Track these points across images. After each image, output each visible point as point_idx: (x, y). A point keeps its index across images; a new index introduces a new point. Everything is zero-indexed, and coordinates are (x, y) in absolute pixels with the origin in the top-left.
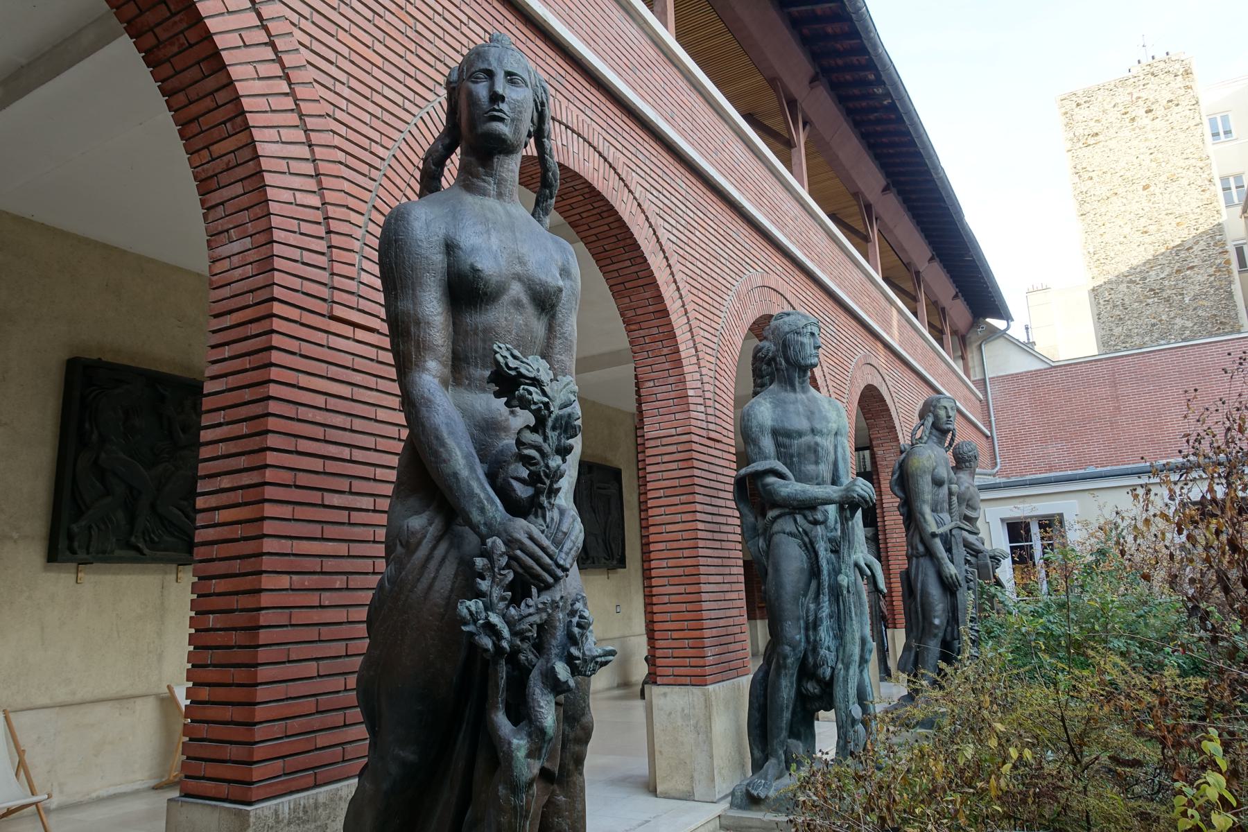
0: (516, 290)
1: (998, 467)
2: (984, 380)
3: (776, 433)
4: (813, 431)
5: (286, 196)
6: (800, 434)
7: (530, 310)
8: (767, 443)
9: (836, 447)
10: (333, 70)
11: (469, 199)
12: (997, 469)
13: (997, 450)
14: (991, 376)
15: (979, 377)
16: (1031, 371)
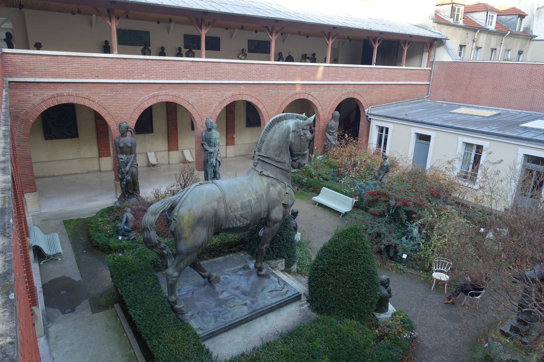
0: (125, 147)
1: (428, 96)
2: (433, 61)
3: (205, 138)
4: (210, 138)
5: (113, 128)
6: (208, 139)
7: (127, 148)
8: (204, 139)
9: (215, 141)
10: (118, 111)
11: (121, 138)
12: (428, 96)
13: (430, 90)
14: (436, 61)
15: (432, 60)
16: (448, 62)
